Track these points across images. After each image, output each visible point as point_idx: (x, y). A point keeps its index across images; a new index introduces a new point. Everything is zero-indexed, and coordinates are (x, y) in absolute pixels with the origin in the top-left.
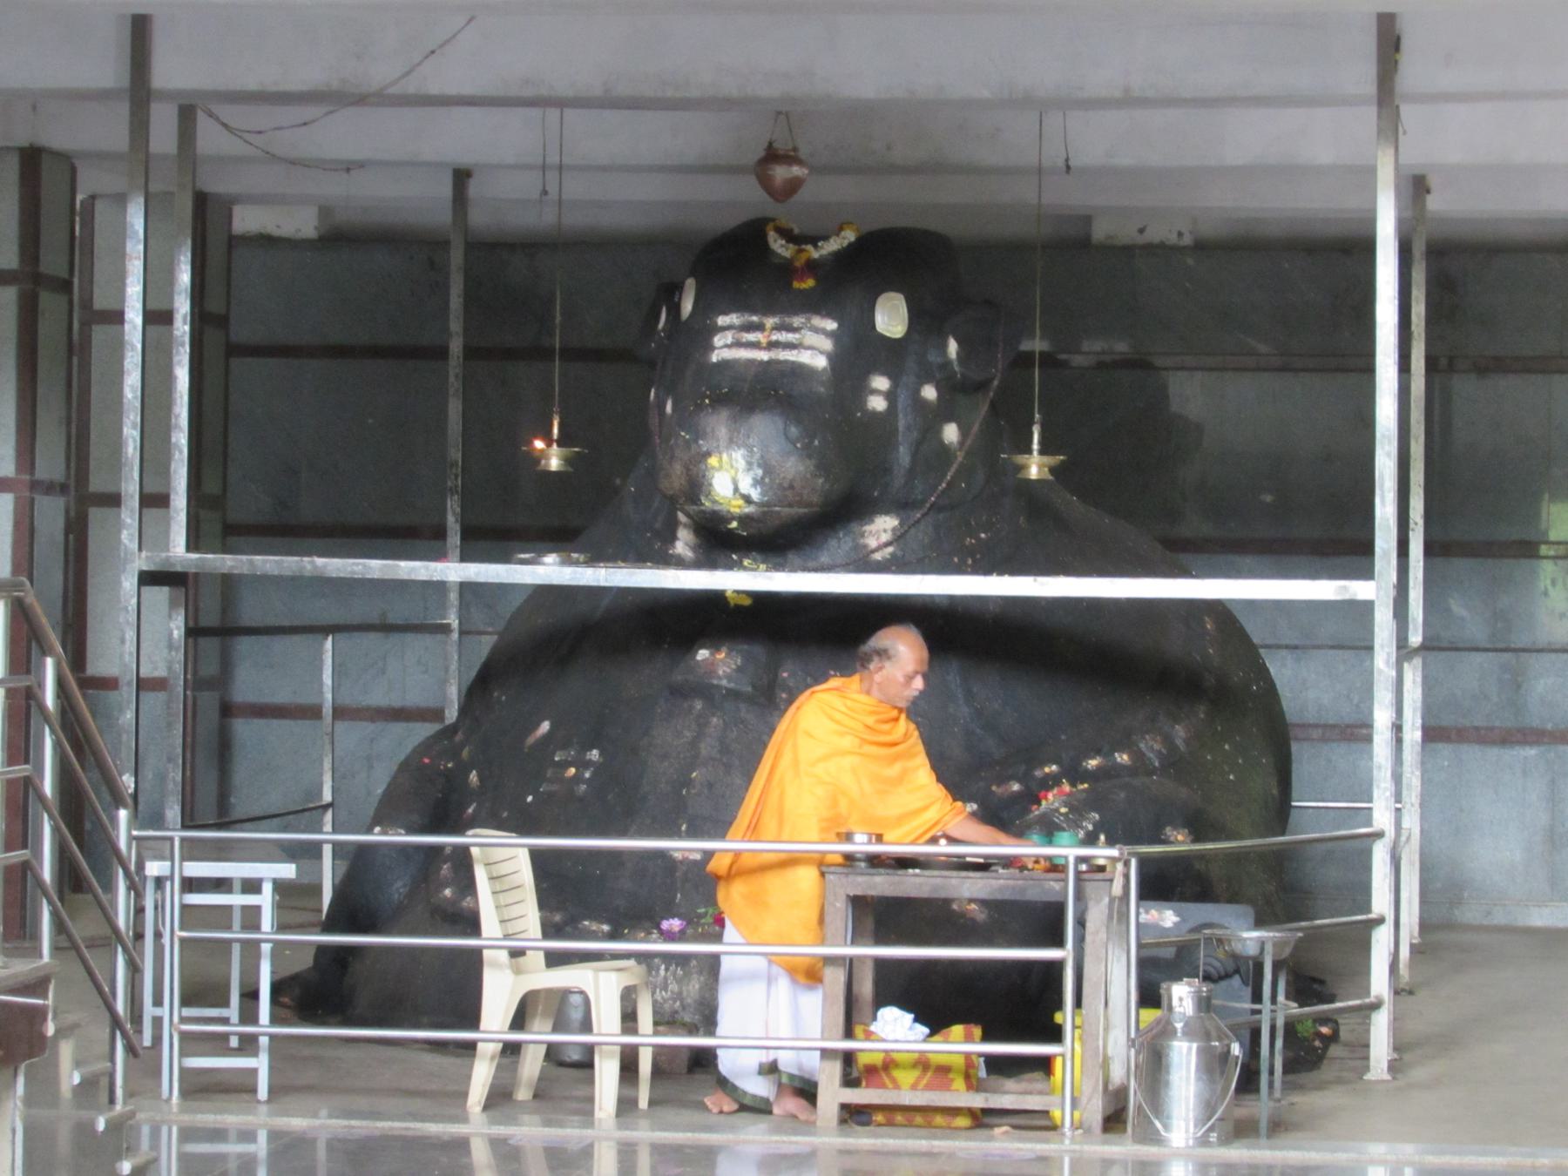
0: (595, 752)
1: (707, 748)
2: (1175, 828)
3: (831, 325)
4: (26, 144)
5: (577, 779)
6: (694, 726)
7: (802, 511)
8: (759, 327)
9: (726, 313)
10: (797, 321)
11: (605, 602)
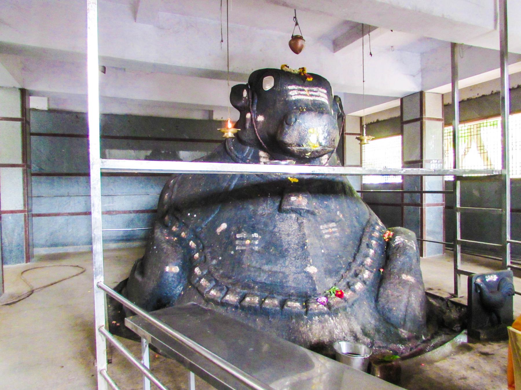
6: (296, 223)
8: (303, 90)
9: (291, 85)
10: (315, 89)
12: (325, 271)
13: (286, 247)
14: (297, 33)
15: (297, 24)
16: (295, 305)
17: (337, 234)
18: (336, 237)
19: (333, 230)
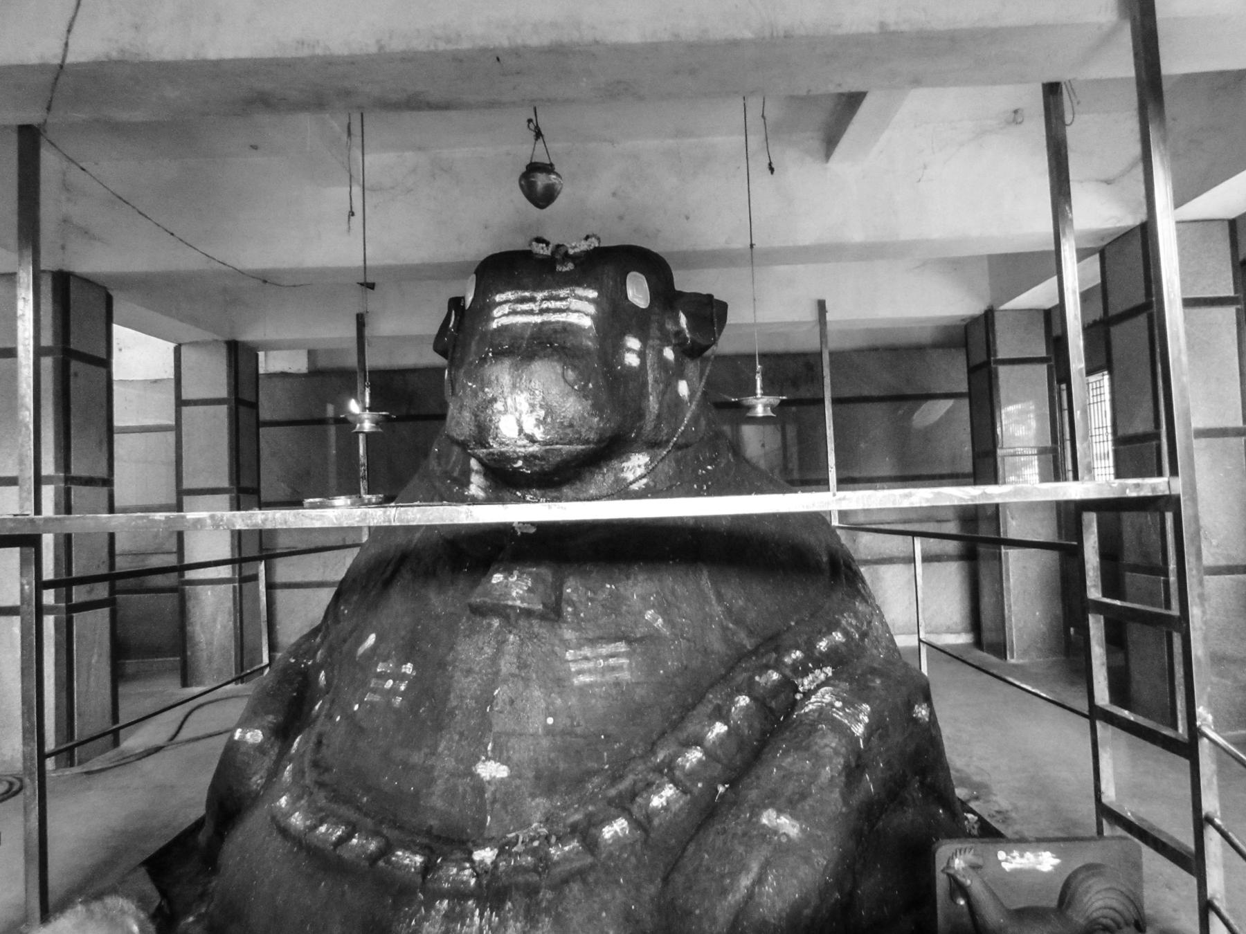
0: (409, 665)
1: (507, 665)
2: (920, 705)
3: (593, 294)
4: (55, 269)
5: (394, 692)
6: (493, 643)
7: (580, 447)
8: (533, 300)
9: (503, 292)
10: (563, 293)
11: (418, 535)
12: (538, 777)
13: (454, 703)
14: (541, 158)
15: (538, 134)
16: (407, 861)
17: (626, 676)
18: (617, 684)
19: (612, 661)
